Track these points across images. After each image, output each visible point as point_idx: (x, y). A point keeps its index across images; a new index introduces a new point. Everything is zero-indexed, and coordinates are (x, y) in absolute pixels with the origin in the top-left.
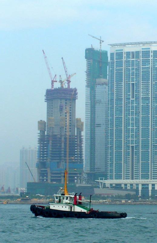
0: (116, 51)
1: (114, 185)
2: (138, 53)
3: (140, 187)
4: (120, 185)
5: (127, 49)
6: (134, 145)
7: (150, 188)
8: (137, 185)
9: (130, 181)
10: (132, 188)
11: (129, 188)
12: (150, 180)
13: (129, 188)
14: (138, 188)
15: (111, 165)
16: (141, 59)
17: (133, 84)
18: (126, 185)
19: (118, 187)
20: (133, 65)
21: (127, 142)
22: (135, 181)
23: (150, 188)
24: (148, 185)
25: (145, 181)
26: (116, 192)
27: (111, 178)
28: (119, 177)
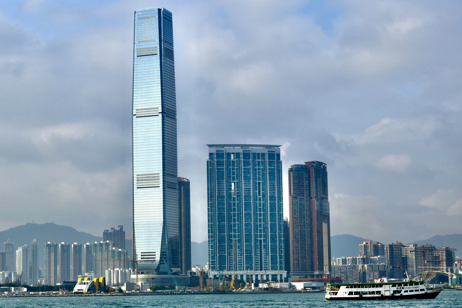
0: (217, 151)
6: (237, 239)
8: (242, 276)
10: (237, 278)
20: (233, 166)
21: (230, 236)
24: (252, 276)
25: (249, 272)
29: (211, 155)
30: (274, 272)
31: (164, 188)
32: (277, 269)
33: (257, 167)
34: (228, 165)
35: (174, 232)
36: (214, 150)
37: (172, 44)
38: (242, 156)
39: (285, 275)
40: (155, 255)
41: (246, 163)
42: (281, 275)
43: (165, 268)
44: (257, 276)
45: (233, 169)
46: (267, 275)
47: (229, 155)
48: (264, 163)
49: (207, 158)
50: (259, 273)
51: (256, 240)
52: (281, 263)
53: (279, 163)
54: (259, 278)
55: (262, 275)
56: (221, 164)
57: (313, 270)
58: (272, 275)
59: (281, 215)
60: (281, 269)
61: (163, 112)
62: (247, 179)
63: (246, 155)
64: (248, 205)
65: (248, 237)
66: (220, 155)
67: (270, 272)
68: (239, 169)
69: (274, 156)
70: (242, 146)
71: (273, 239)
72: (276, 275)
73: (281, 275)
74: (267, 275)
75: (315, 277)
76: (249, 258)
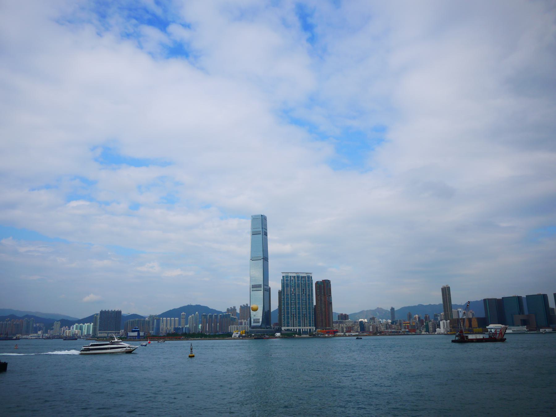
5: (290, 275)
9: (292, 328)
19: (288, 330)
22: (295, 328)
27: (284, 326)
28: (288, 326)
29: (283, 277)
30: (310, 328)
34: (291, 281)
35: (266, 310)
36: (284, 275)
37: (266, 230)
39: (314, 329)
41: (298, 280)
43: (264, 326)
47: (291, 277)
48: (305, 280)
49: (282, 278)
50: (304, 328)
53: (312, 280)
56: (287, 281)
59: (312, 303)
62: (298, 287)
63: (298, 277)
64: (299, 298)
65: (299, 314)
66: (287, 277)
68: (295, 283)
69: (310, 278)
70: (296, 273)
71: (310, 314)
76: (299, 322)
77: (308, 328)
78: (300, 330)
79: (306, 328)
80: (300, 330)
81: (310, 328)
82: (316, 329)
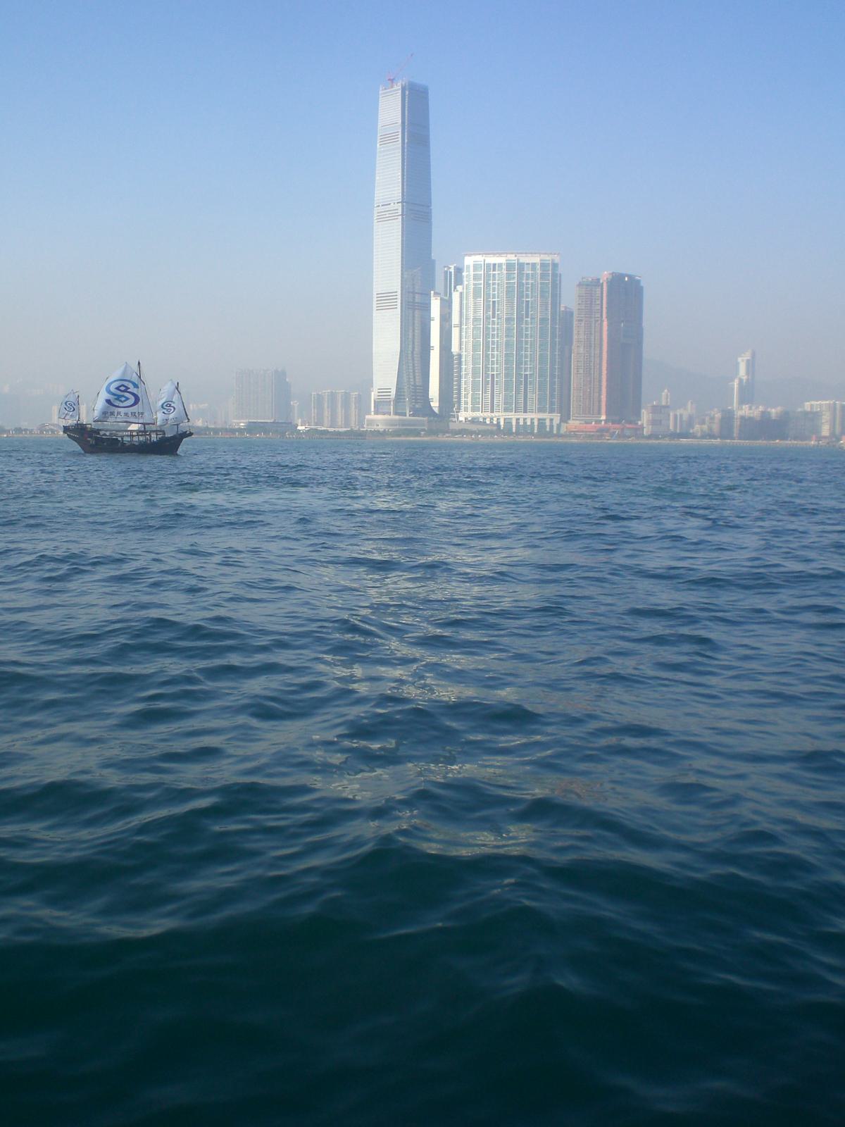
1: (470, 419)
2: (500, 265)
3: (502, 423)
4: (478, 418)
6: (495, 373)
7: (514, 423)
11: (488, 421)
12: (513, 413)
13: (488, 421)
14: (498, 423)
15: (466, 396)
16: (505, 272)
17: (494, 302)
18: (485, 419)
20: (494, 280)
23: (514, 423)
26: (474, 427)
27: (466, 410)
28: (474, 410)
30: (541, 416)
31: (401, 310)
32: (545, 412)
33: (524, 281)
38: (504, 267)
40: (390, 392)
42: (551, 420)
44: (518, 419)
45: (494, 284)
46: (532, 419)
50: (521, 416)
51: (518, 375)
52: (552, 403)
54: (521, 423)
55: (525, 419)
57: (599, 413)
58: (539, 420)
60: (552, 411)
61: (402, 215)
67: (536, 416)
72: (545, 419)
73: (551, 420)
74: (532, 419)
75: (603, 423)
77: (536, 416)
78: (508, 422)
79: (529, 416)
80: (508, 422)
81: (541, 416)
82: (562, 420)
